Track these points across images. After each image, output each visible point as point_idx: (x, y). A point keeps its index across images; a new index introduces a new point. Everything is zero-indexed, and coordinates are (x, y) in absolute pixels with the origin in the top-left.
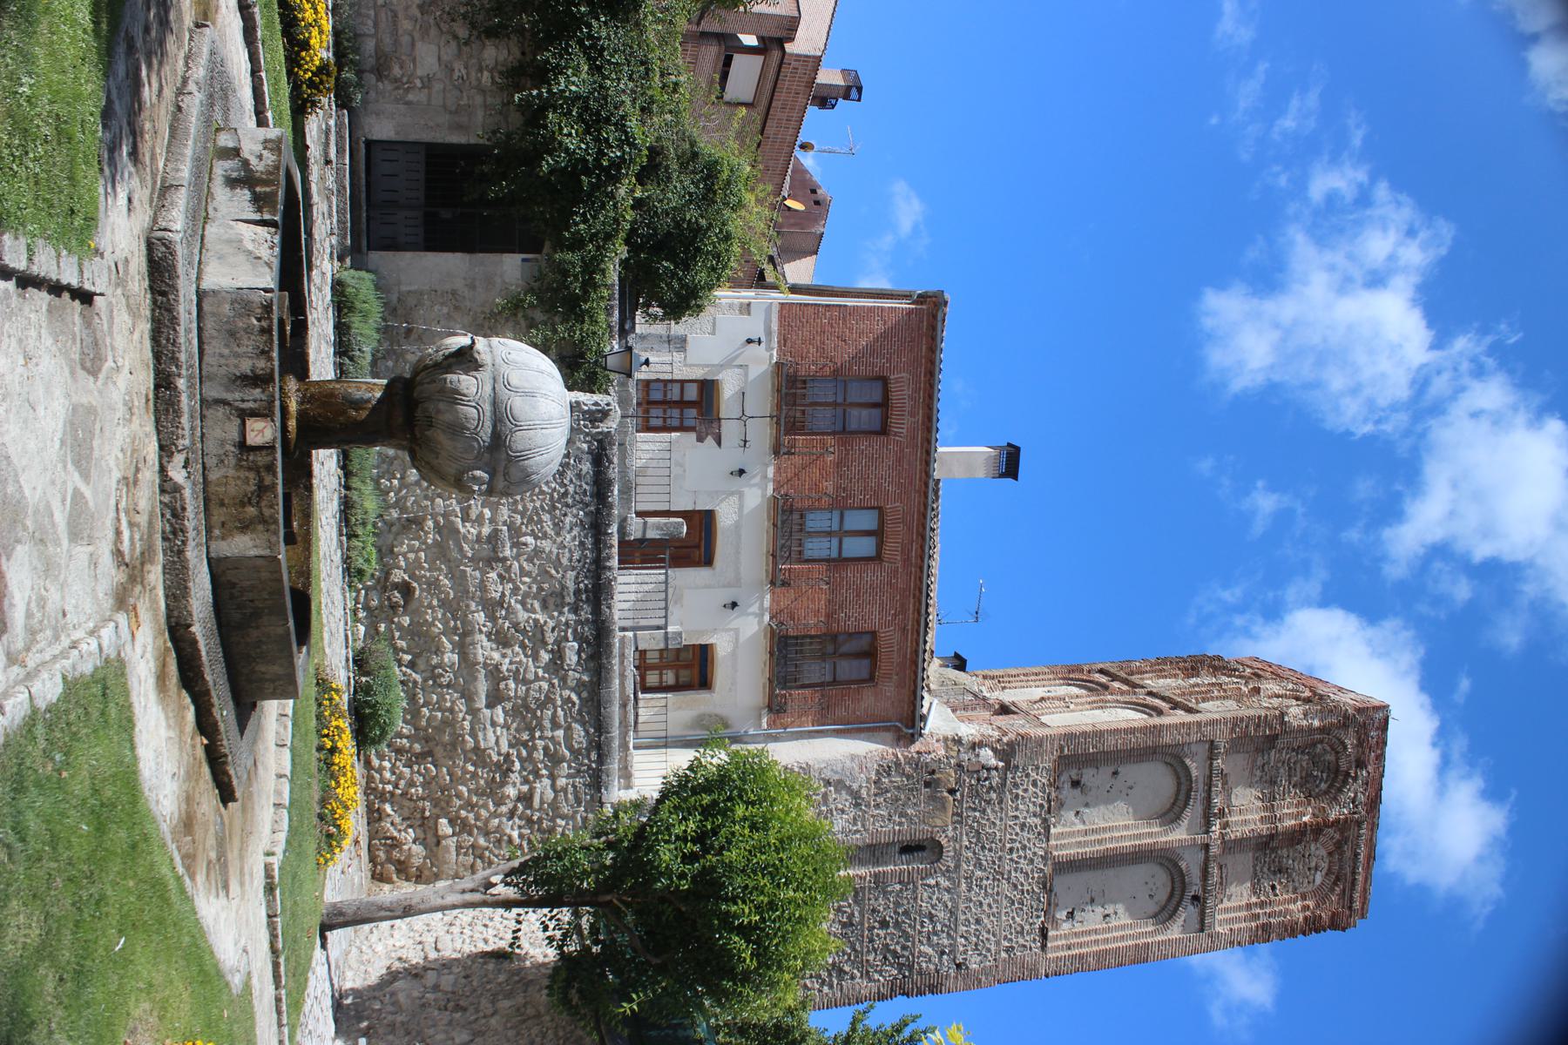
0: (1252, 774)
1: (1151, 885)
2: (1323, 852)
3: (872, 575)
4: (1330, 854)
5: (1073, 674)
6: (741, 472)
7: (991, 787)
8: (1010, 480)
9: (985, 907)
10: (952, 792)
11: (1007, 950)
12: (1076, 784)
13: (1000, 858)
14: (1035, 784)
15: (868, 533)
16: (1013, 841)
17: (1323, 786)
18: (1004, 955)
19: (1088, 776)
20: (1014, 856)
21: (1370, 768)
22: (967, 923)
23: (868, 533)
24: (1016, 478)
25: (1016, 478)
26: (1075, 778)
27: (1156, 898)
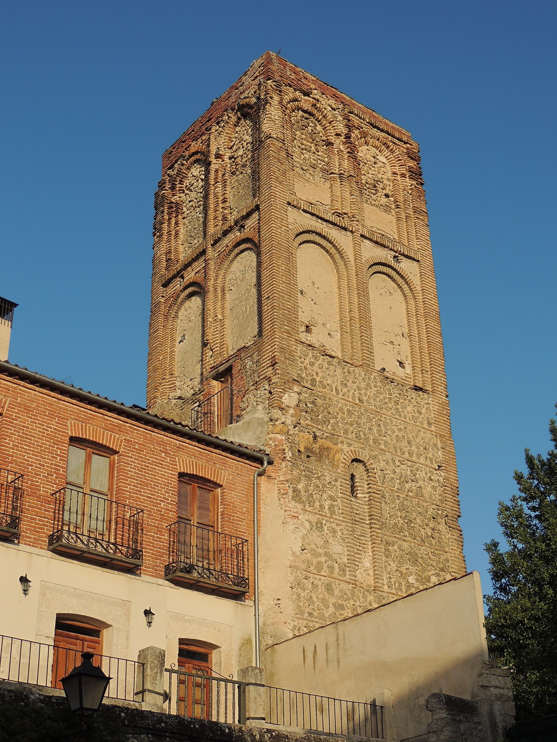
0: (307, 181)
1: (383, 291)
2: (365, 147)
3: (130, 463)
4: (367, 143)
5: (159, 314)
6: (24, 580)
7: (313, 403)
8: (16, 309)
9: (400, 434)
10: (315, 437)
11: (429, 424)
12: (308, 329)
13: (366, 411)
14: (312, 364)
15: (88, 460)
16: (353, 397)
17: (319, 128)
18: (433, 428)
19: (304, 317)
20: (365, 398)
21: (313, 86)
22: (411, 454)
23: (88, 460)
24: (16, 305)
25: (16, 305)
26: (303, 328)
27: (392, 291)
